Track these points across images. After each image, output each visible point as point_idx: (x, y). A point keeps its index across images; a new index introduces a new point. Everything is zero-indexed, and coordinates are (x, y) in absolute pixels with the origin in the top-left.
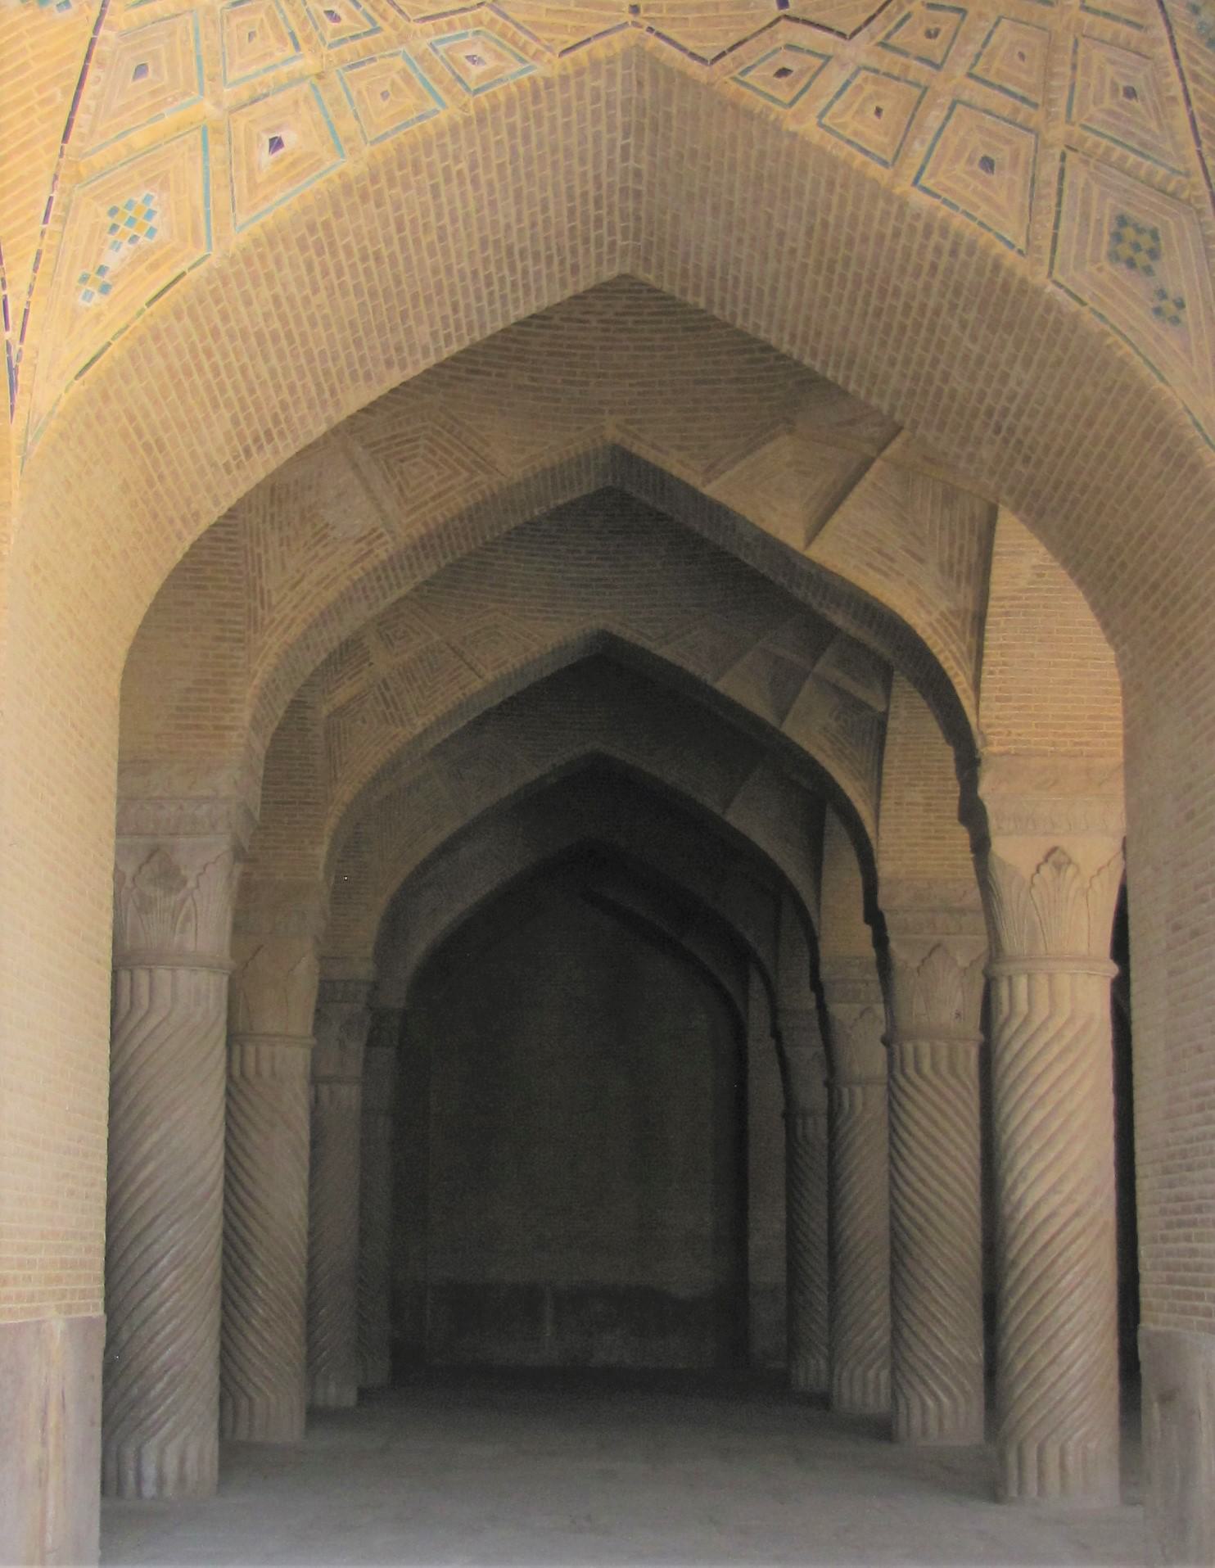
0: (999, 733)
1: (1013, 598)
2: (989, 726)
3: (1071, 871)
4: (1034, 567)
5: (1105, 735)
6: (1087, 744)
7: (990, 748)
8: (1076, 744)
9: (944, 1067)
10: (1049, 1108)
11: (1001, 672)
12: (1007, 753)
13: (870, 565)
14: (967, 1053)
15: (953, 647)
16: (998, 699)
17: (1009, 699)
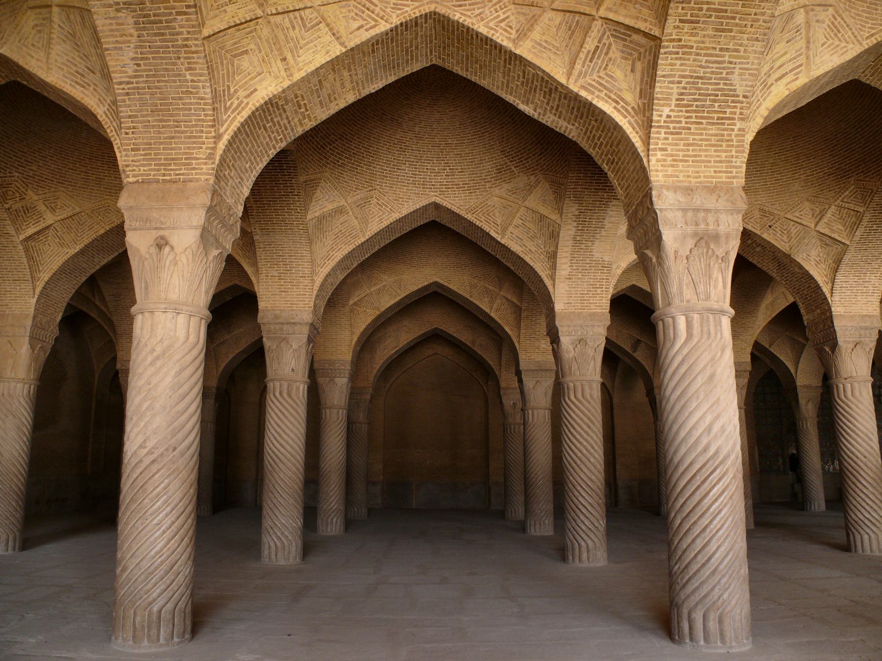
0: (134, 170)
1: (128, 83)
2: (127, 166)
3: (167, 249)
4: (133, 59)
5: (194, 169)
6: (183, 174)
7: (128, 180)
8: (177, 175)
9: (285, 395)
10: (143, 395)
11: (133, 133)
12: (137, 182)
13: (76, 83)
14: (298, 389)
15: (114, 124)
16: (133, 150)
17: (139, 150)
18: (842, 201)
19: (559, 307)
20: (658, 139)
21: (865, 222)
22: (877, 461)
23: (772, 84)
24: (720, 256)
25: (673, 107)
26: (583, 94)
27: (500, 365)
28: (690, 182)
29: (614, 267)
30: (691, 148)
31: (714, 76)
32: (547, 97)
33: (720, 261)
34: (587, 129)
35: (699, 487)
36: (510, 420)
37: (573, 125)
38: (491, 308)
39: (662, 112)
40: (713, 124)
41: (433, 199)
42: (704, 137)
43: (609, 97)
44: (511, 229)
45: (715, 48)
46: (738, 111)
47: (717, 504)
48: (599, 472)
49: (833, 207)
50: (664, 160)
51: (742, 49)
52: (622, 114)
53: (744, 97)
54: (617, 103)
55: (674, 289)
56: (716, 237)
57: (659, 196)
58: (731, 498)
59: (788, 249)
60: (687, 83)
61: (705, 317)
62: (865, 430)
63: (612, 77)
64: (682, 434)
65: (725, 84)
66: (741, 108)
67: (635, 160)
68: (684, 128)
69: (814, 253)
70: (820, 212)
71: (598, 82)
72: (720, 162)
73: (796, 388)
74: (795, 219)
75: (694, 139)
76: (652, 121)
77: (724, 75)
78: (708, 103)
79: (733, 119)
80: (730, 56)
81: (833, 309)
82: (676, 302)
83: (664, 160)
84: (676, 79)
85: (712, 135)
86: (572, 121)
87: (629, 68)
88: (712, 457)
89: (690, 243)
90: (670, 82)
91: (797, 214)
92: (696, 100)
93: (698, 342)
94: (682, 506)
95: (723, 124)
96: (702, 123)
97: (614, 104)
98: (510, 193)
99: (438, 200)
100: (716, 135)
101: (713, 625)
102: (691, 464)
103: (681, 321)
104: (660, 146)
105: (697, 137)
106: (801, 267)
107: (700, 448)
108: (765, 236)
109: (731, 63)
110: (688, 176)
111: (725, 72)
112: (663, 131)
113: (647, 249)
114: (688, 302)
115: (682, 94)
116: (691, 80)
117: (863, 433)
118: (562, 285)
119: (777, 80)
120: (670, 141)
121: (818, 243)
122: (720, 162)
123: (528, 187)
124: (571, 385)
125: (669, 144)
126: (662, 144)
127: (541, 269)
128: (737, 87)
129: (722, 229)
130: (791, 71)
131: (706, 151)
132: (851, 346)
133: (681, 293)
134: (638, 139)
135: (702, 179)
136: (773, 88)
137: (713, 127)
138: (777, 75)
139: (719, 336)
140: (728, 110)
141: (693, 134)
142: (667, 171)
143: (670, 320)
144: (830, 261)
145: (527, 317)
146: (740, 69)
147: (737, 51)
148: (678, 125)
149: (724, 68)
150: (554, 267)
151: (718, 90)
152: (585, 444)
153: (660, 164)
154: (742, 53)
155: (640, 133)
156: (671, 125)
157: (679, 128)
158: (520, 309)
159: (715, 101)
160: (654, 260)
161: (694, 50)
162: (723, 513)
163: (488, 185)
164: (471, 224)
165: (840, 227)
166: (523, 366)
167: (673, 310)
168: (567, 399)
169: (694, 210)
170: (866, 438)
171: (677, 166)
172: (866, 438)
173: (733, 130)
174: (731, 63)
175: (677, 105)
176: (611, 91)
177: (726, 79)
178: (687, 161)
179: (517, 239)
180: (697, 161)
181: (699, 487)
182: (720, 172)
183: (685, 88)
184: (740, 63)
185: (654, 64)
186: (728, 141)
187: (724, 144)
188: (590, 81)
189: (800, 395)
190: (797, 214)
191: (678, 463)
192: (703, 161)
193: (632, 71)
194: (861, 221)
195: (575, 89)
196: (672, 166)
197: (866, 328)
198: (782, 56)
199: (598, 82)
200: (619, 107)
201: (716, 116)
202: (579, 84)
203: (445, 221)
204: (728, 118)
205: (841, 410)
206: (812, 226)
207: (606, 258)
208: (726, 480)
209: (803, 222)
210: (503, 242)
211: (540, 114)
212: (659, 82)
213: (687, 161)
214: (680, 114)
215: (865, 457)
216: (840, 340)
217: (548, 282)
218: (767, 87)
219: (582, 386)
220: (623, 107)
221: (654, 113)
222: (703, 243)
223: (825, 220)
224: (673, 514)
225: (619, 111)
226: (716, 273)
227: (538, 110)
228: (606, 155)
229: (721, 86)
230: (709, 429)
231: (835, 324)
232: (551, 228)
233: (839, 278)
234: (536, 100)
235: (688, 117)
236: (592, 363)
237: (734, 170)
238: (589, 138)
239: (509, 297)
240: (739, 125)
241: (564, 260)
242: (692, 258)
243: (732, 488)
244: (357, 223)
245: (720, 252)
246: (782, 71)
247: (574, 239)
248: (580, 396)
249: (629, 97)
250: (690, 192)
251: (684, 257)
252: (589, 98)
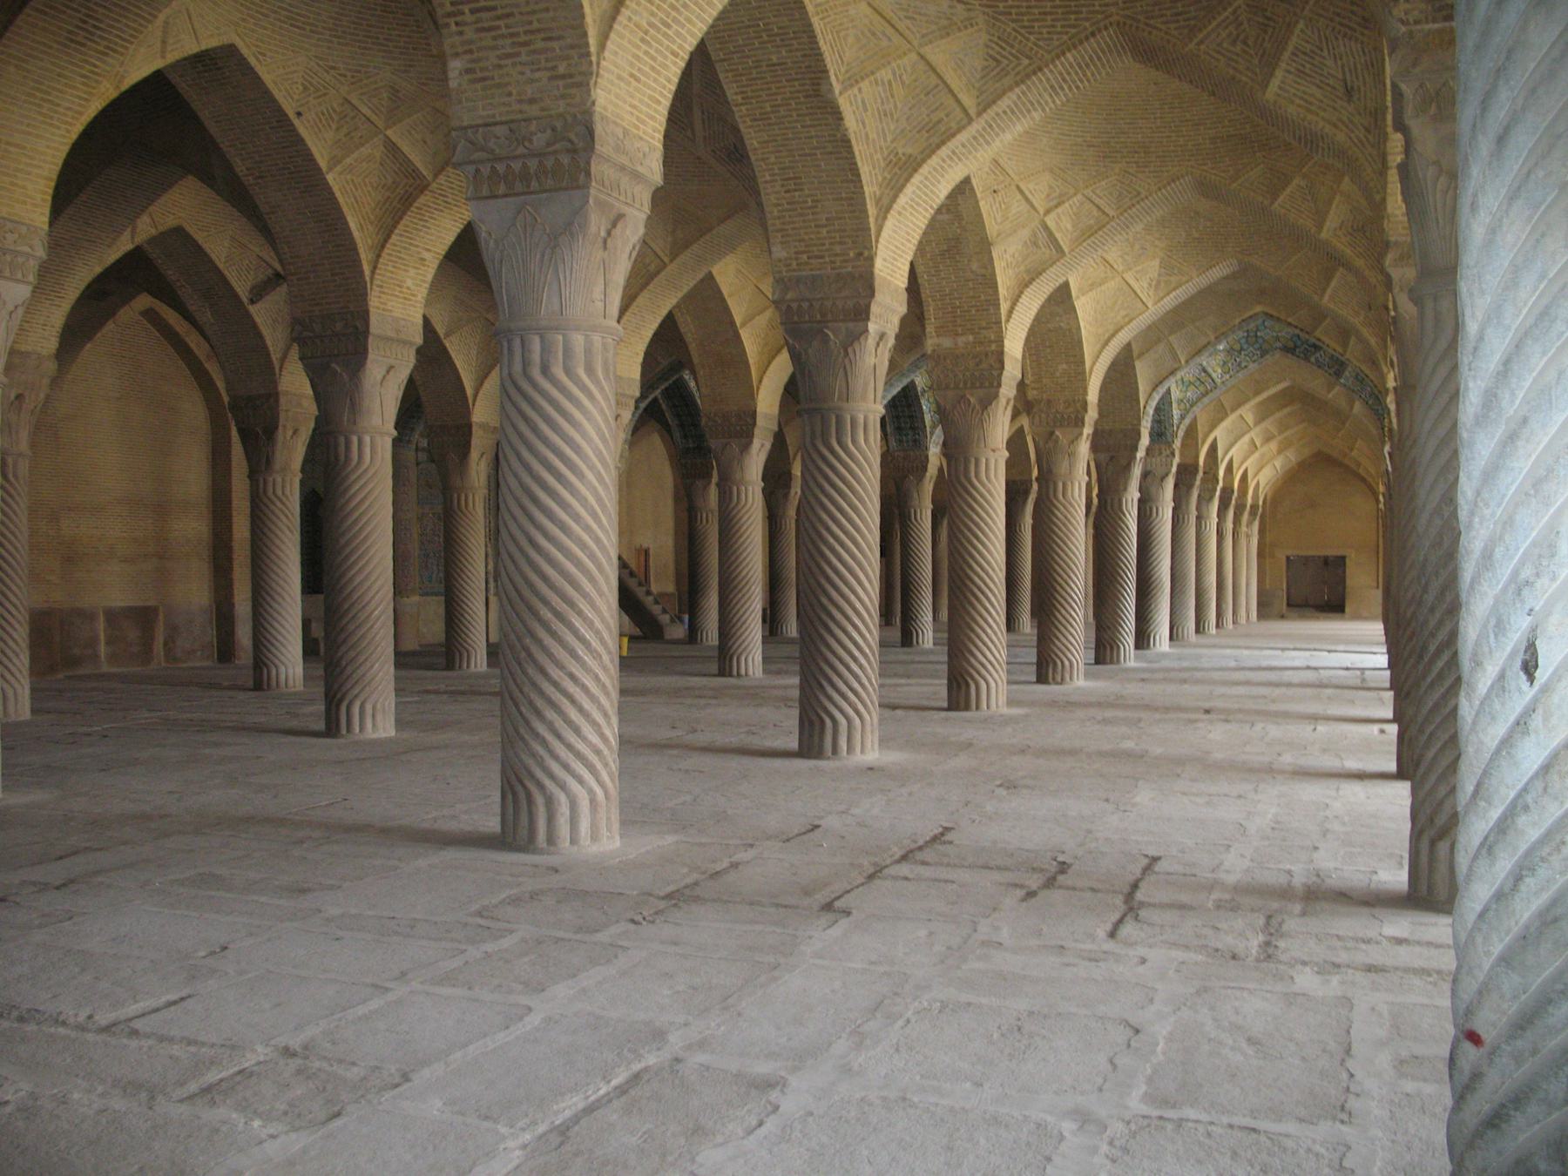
44: (865, 85)
49: (1079, 196)
73: (470, 426)
98: (901, 14)
123: (946, 22)
165: (1069, 226)
190: (1031, 186)
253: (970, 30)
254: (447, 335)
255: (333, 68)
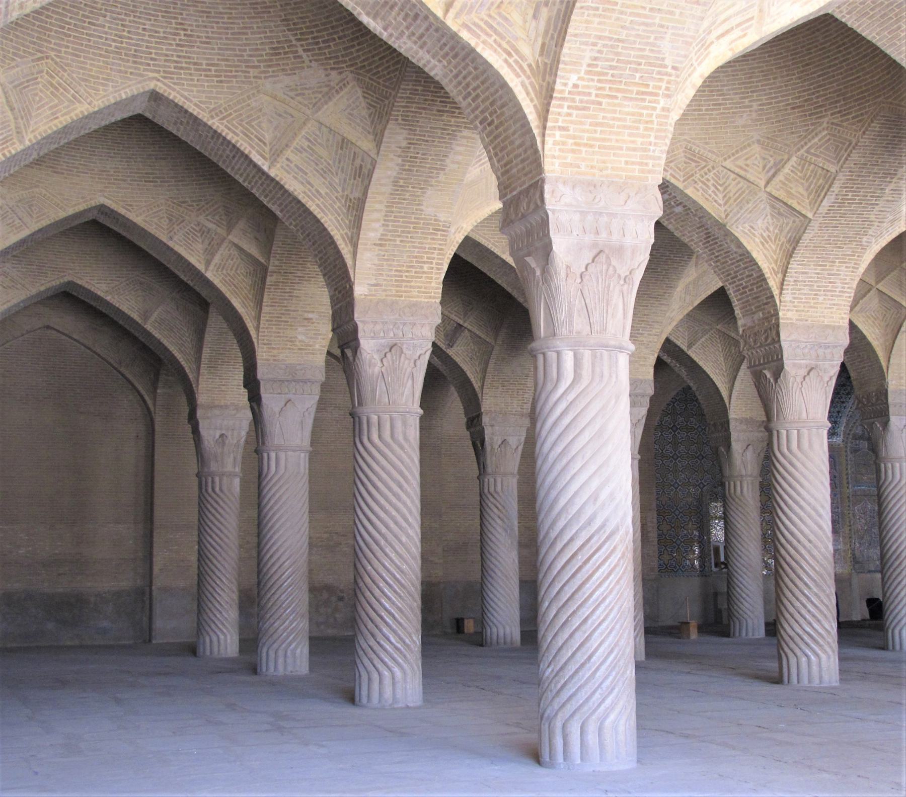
18: (808, 152)
19: (359, 290)
20: (559, 114)
21: (836, 188)
22: (826, 548)
23: (712, 43)
24: (623, 276)
25: (582, 74)
26: (465, 35)
27: (198, 360)
28: (594, 175)
29: (452, 230)
30: (599, 129)
31: (638, 40)
32: (409, 20)
33: (622, 282)
34: (460, 72)
35: (580, 568)
36: (213, 467)
37: (440, 61)
38: (208, 263)
39: (568, 80)
40: (631, 99)
41: (152, 85)
42: (618, 115)
43: (500, 46)
44: (288, 153)
45: (644, 8)
46: (664, 85)
47: (602, 589)
48: (414, 558)
49: (794, 159)
50: (564, 143)
51: (677, 11)
52: (514, 70)
53: (674, 68)
54: (509, 54)
55: (561, 315)
56: (619, 250)
57: (553, 192)
58: (618, 582)
59: (723, 216)
60: (604, 46)
61: (598, 354)
62: (812, 501)
63: (506, 19)
64: (562, 502)
65: (652, 51)
66: (669, 82)
67: (524, 135)
68: (593, 103)
69: (760, 224)
70: (775, 164)
71: (486, 23)
72: (634, 150)
74: (737, 170)
75: (604, 118)
76: (553, 90)
77: (651, 40)
78: (627, 72)
79: (656, 95)
80: (662, 19)
81: (781, 314)
82: (563, 331)
83: (564, 143)
84: (591, 40)
85: (628, 114)
86: (439, 57)
87: (531, 12)
88: (597, 531)
89: (588, 256)
90: (582, 43)
91: (740, 162)
92: (612, 68)
93: (589, 384)
94: (558, 593)
95: (643, 100)
96: (616, 97)
97: (505, 56)
98: (292, 94)
99: (161, 88)
100: (633, 114)
101: (592, 738)
102: (571, 540)
103: (568, 359)
104: (560, 124)
105: (609, 115)
106: (740, 245)
107: (583, 519)
108: (689, 192)
109: (662, 26)
110: (592, 167)
111: (653, 37)
112: (566, 104)
113: (529, 255)
114: (578, 333)
115: (596, 59)
116: (610, 43)
117: (809, 504)
118: (368, 255)
119: (718, 38)
120: (574, 118)
121: (768, 209)
122: (634, 150)
123: (326, 89)
124: (374, 418)
125: (572, 122)
126: (564, 121)
127: (335, 225)
128: (667, 55)
129: (628, 241)
130: (738, 25)
131: (618, 133)
132: (803, 372)
133: (571, 322)
134: (532, 109)
135: (609, 172)
136: (711, 49)
137: (630, 103)
138: (720, 31)
139: (614, 379)
140: (651, 84)
141: (603, 110)
142: (565, 158)
143: (554, 355)
144: (783, 239)
145: (276, 284)
146: (673, 34)
147: (671, 13)
148: (586, 98)
149: (652, 32)
150: (356, 224)
151: (642, 57)
152: (394, 513)
153: (558, 147)
154: (677, 17)
155: (536, 102)
156: (578, 98)
157: (587, 102)
158: (265, 269)
159: (636, 70)
160: (538, 273)
161: (618, 7)
162: (608, 601)
163: (253, 72)
164: (216, 134)
165: (801, 190)
166: (262, 372)
167: (558, 344)
168: (365, 440)
169: (595, 213)
170: (813, 513)
171: (580, 152)
172: (813, 513)
173: (654, 109)
174: (662, 26)
175: (588, 73)
176: (503, 38)
177: (653, 45)
178: (591, 146)
179: (299, 176)
180: (605, 147)
181: (580, 568)
182: (633, 163)
183: (599, 52)
184: (673, 28)
185: (564, 16)
186: (647, 122)
187: (642, 126)
188: (477, 20)
189: (734, 436)
190: (740, 162)
191: (556, 538)
192: (613, 148)
193: (535, 17)
194: (830, 186)
195: (454, 28)
196: (573, 151)
197: (827, 347)
198: (729, 8)
199: (486, 23)
200: (511, 61)
201: (635, 89)
202: (460, 22)
203: (163, 118)
204: (651, 94)
205: (781, 469)
206: (762, 183)
207: (442, 217)
208: (613, 560)
209: (748, 176)
210: (272, 174)
211: (391, 35)
212: (569, 41)
213: (591, 146)
214: (591, 83)
215: (810, 541)
216: (788, 362)
217: (345, 250)
218: (705, 46)
219: (392, 419)
220: (516, 62)
221: (558, 81)
222: (602, 257)
223: (780, 177)
224: (546, 604)
225: (510, 66)
226: (617, 300)
227: (390, 30)
228: (483, 112)
229: (646, 53)
230: (595, 497)
231: (782, 337)
232: (358, 162)
233: (794, 266)
234: (391, 18)
235: (600, 89)
236: (410, 382)
237: (651, 162)
238: (460, 83)
239: (245, 247)
240: (662, 102)
241: (375, 215)
242: (587, 277)
243: (620, 571)
244: (11, 117)
245: (623, 271)
246: (726, 27)
247: (395, 183)
248: (387, 435)
249: (526, 50)
250: (592, 188)
251: (578, 276)
252: (473, 43)
253: (346, 90)
254: (689, 347)
255: (184, 202)
